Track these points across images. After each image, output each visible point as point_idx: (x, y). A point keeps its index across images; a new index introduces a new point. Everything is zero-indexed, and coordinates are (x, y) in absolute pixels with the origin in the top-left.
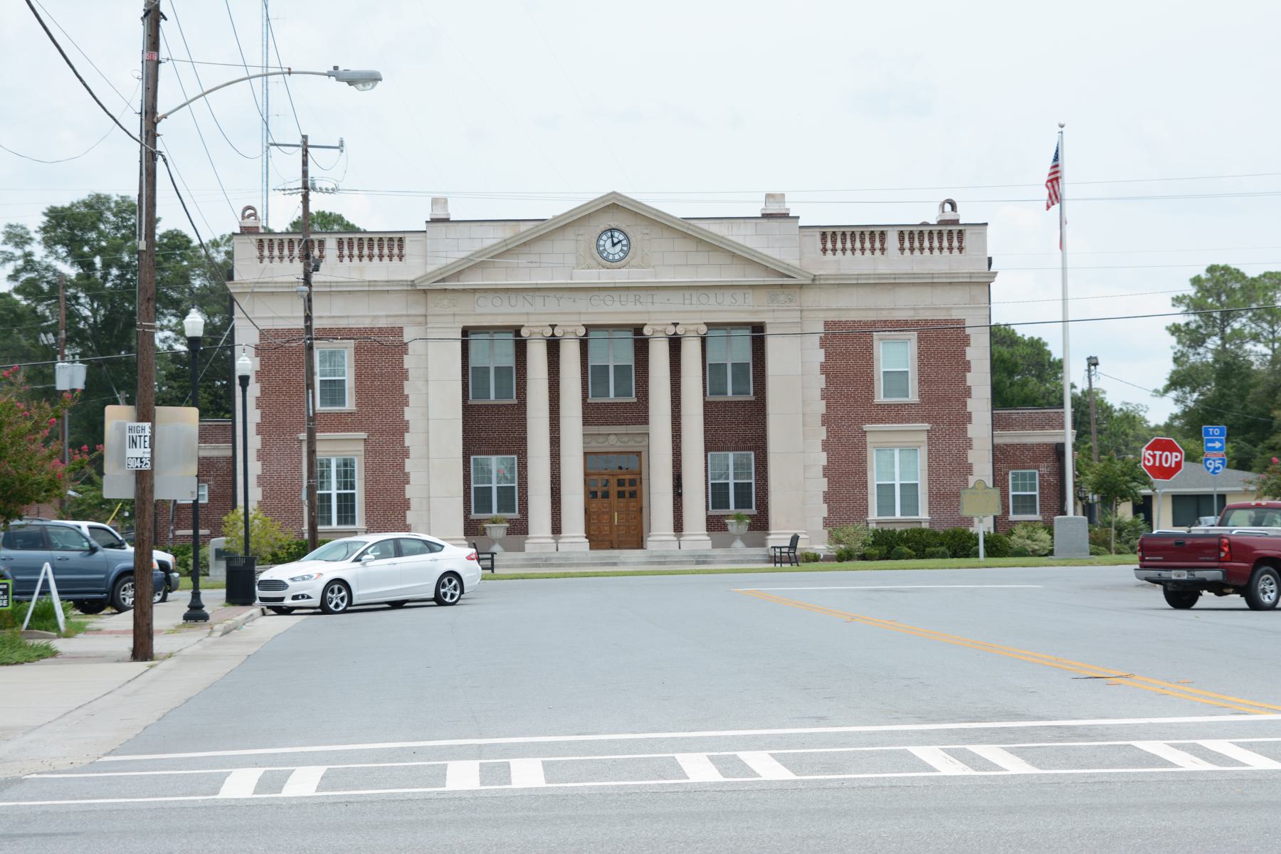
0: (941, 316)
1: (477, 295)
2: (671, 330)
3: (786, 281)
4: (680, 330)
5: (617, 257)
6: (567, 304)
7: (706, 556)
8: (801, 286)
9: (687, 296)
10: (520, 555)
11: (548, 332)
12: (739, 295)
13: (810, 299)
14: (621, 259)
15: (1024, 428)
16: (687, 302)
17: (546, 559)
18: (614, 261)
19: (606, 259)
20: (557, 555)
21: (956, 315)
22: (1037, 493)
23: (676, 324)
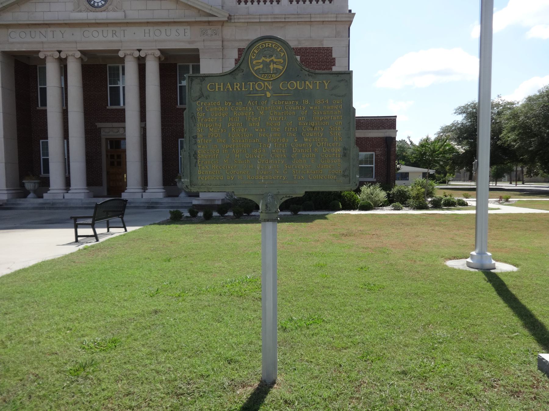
0: (316, 45)
1: (10, 30)
2: (137, 54)
3: (211, 19)
4: (142, 54)
5: (100, 4)
6: (69, 34)
7: (157, 203)
8: (222, 23)
9: (147, 31)
10: (40, 201)
11: (57, 55)
12: (181, 29)
13: (229, 32)
14: (103, 5)
15: (367, 129)
16: (147, 35)
17: (53, 204)
18: (98, 7)
19: (93, 6)
20: (64, 201)
21: (326, 44)
22: (374, 166)
23: (139, 50)
